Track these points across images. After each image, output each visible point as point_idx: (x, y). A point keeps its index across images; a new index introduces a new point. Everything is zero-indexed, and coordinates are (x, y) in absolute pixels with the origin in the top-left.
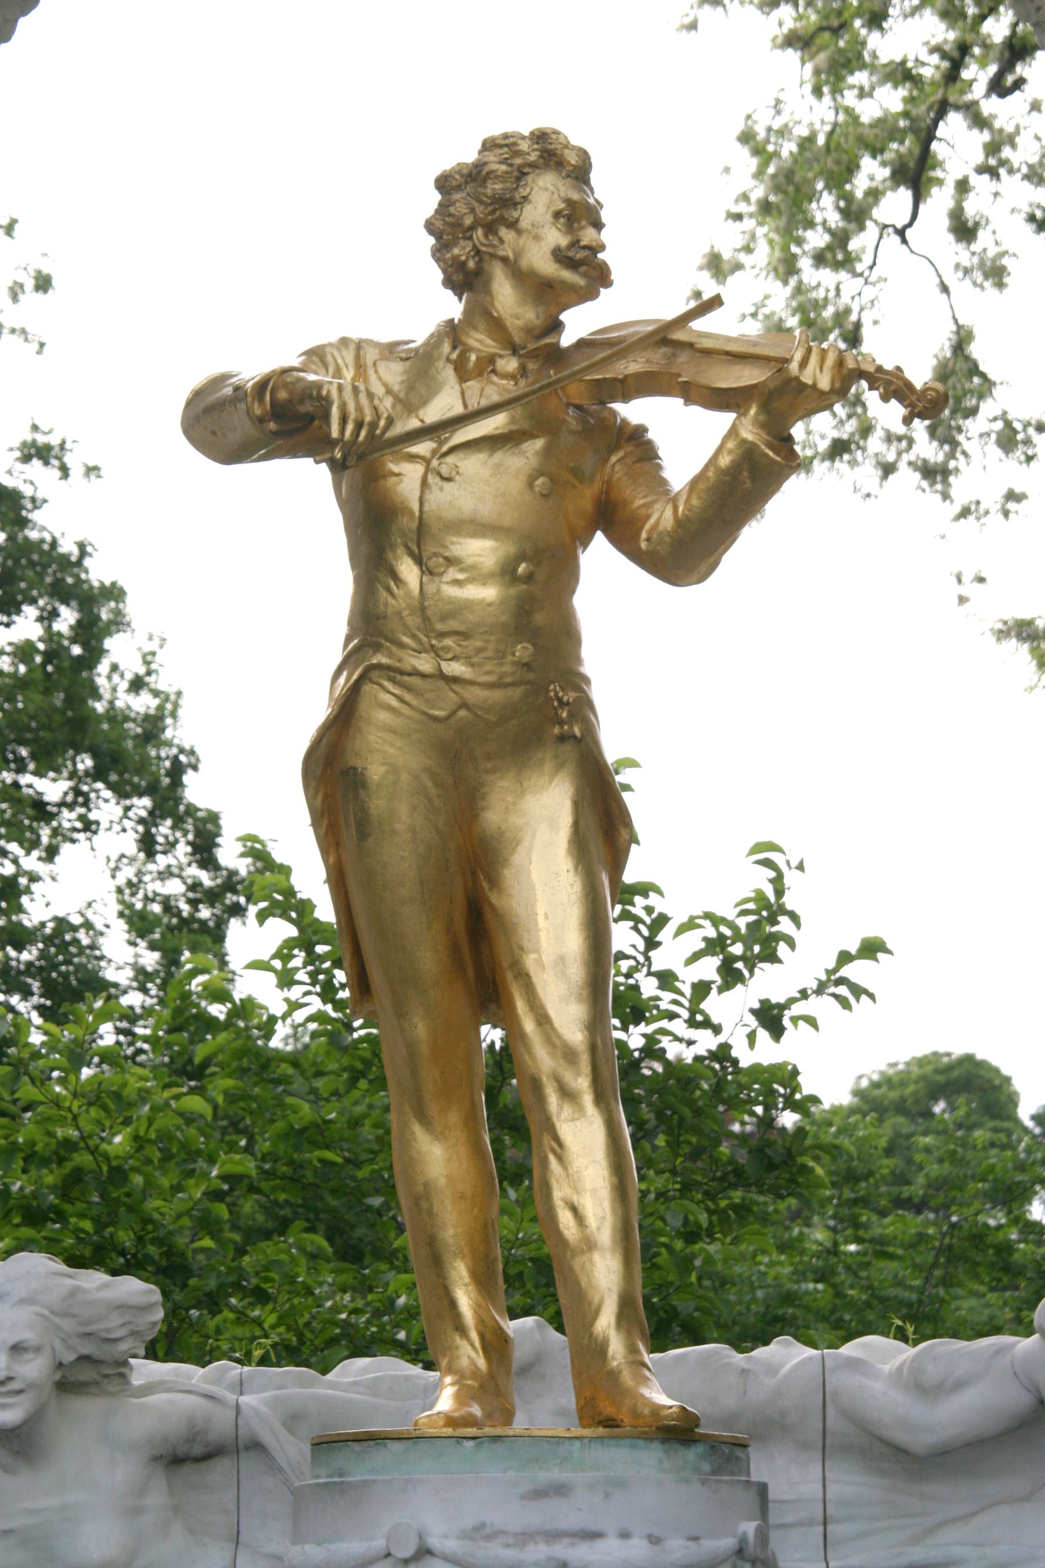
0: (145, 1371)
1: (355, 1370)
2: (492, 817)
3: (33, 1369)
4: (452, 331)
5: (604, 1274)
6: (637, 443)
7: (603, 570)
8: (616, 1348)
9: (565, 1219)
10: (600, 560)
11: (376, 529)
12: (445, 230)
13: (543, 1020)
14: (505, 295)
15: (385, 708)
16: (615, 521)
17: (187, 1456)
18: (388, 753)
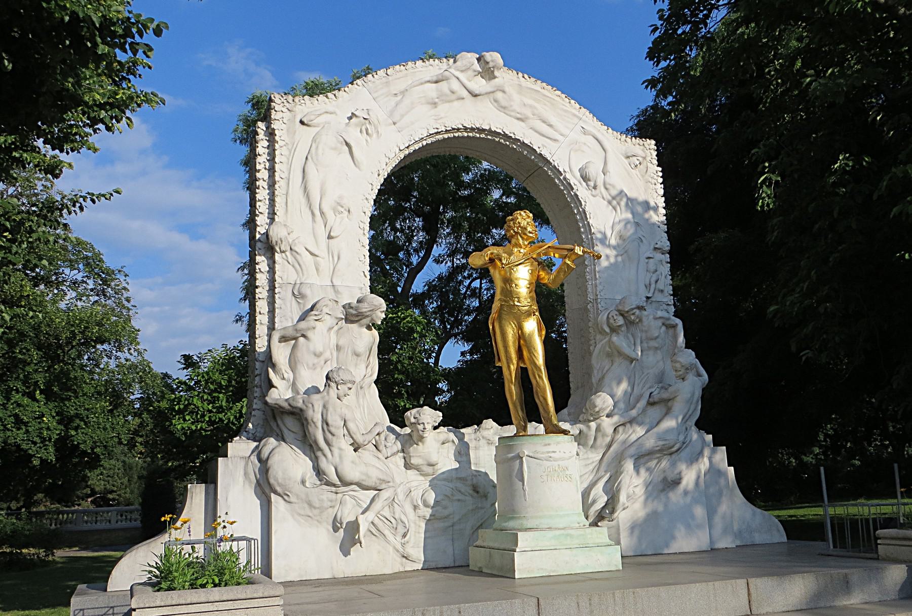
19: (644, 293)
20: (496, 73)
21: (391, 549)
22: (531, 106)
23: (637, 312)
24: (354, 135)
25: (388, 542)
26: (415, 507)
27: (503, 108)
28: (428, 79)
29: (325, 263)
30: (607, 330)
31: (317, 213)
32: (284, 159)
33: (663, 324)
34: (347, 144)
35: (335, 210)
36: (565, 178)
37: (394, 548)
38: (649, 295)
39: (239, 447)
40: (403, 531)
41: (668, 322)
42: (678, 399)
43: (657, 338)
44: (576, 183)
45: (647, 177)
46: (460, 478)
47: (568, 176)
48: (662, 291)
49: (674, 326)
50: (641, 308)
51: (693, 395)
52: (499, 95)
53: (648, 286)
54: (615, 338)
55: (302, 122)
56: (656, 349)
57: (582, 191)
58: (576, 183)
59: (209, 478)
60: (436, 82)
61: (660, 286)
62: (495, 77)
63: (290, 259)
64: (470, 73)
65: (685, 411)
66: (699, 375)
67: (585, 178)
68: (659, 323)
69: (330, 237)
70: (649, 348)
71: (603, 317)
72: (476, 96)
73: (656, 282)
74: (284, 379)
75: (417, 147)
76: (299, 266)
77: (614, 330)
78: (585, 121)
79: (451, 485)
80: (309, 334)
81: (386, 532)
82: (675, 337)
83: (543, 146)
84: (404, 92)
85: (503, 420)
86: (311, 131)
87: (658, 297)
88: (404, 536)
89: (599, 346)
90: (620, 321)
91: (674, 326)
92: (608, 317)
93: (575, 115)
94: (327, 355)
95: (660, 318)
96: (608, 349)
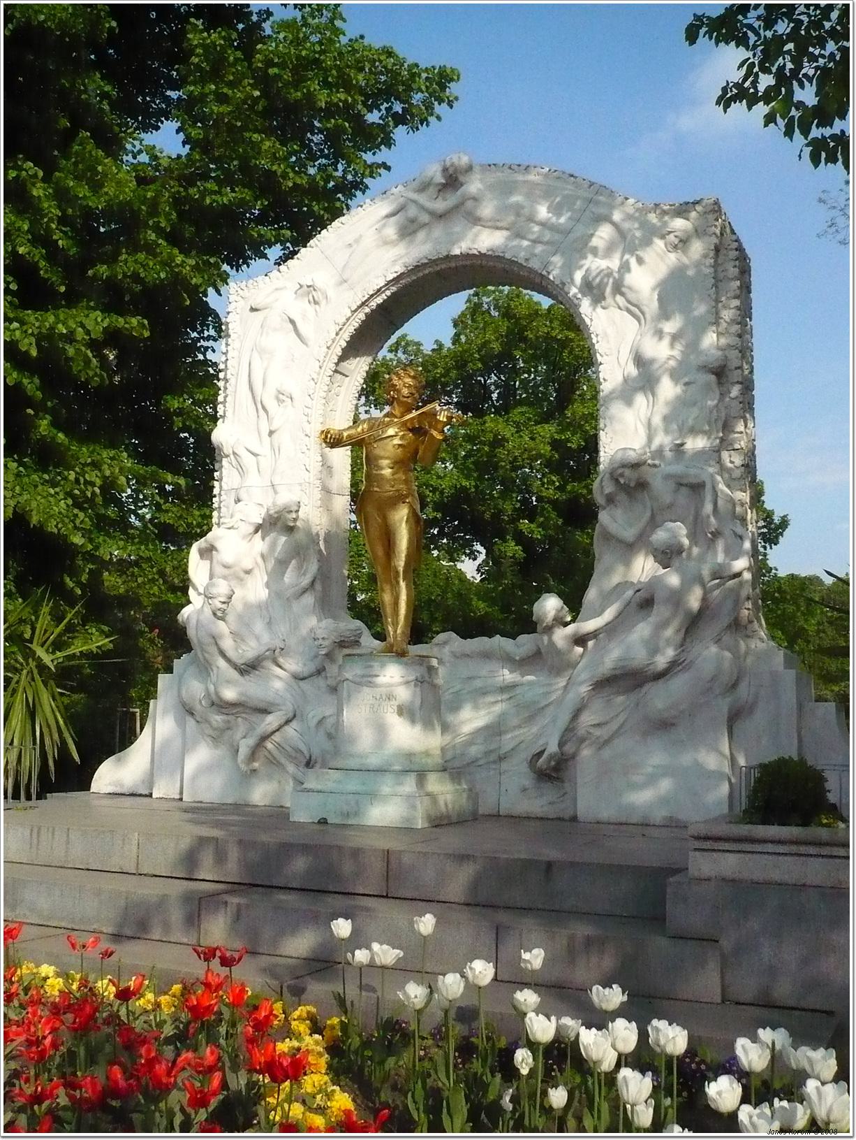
3: (326, 643)
20: (461, 178)
23: (627, 472)
29: (265, 462)
34: (292, 322)
35: (278, 399)
41: (685, 481)
55: (253, 310)
63: (234, 462)
64: (432, 190)
68: (671, 485)
69: (271, 433)
72: (441, 216)
75: (379, 300)
76: (241, 470)
78: (598, 203)
81: (283, 760)
84: (357, 241)
90: (609, 488)
94: (248, 564)
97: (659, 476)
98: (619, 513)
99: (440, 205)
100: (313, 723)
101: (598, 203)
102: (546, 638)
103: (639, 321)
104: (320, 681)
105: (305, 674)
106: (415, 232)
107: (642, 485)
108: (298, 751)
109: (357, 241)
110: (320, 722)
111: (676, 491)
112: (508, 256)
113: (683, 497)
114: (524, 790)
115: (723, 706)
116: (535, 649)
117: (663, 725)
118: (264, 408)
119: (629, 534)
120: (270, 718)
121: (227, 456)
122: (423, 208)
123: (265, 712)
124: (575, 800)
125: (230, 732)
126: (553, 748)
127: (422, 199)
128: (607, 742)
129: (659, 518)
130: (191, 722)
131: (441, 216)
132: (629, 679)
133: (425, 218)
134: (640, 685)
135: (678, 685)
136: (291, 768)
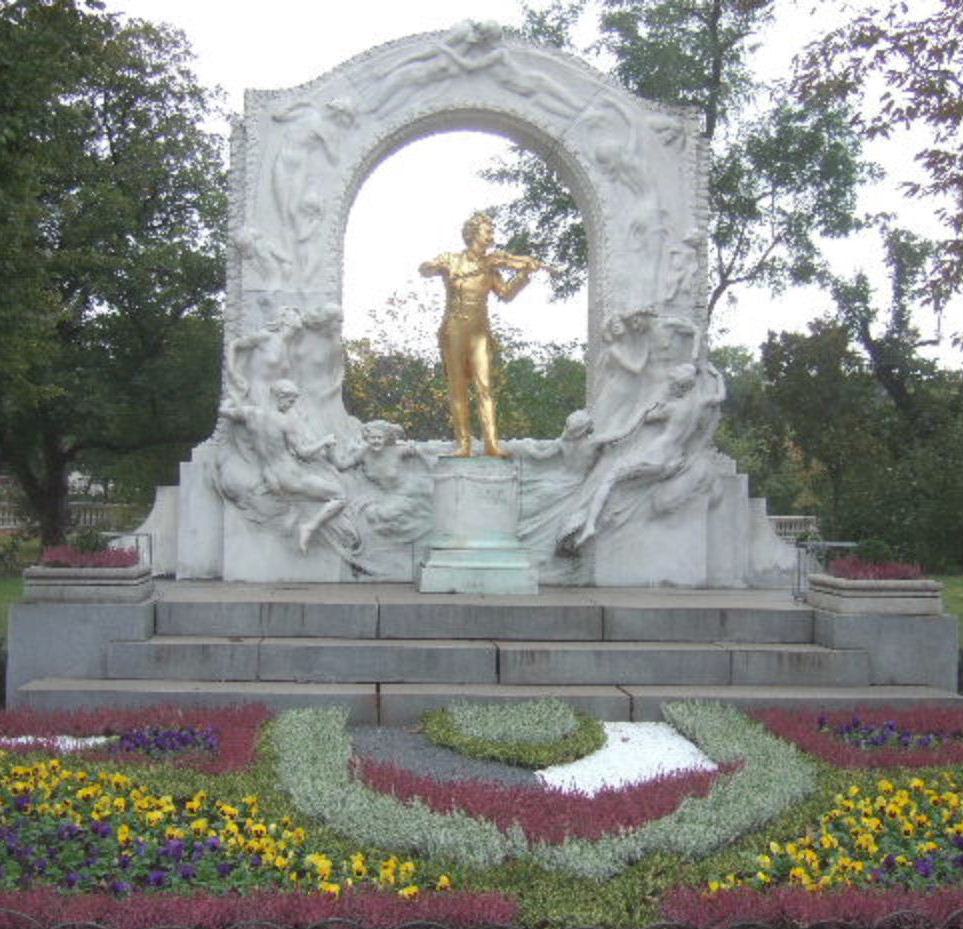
0: (398, 442)
1: (431, 442)
2: (473, 344)
3: (381, 441)
4: (465, 252)
5: (491, 430)
6: (498, 275)
7: (492, 297)
8: (493, 442)
9: (484, 420)
10: (492, 297)
11: (453, 292)
12: (465, 233)
13: (480, 383)
14: (476, 246)
15: (453, 322)
16: (494, 289)
17: (407, 457)
18: (454, 332)
19: (664, 295)
21: (338, 560)
22: (540, 79)
23: (640, 320)
24: (326, 129)
25: (335, 551)
26: (371, 521)
27: (506, 84)
28: (413, 55)
30: (609, 337)
31: (285, 215)
32: (254, 159)
33: (676, 332)
34: (318, 138)
36: (578, 162)
37: (343, 557)
38: (670, 296)
39: (201, 451)
40: (352, 543)
42: (672, 420)
43: (666, 349)
44: (588, 165)
45: (684, 154)
46: (423, 495)
47: (578, 157)
48: (687, 292)
49: (690, 335)
50: (645, 315)
51: (689, 414)
52: (498, 69)
53: (668, 287)
54: (616, 350)
55: (276, 119)
56: (667, 360)
57: (594, 176)
58: (588, 165)
59: (174, 480)
60: (424, 59)
61: (685, 285)
62: (493, 48)
64: (463, 47)
65: (680, 432)
66: (717, 391)
67: (601, 160)
68: (670, 331)
70: (659, 360)
71: (606, 320)
72: (471, 72)
73: (680, 281)
74: (239, 389)
77: (618, 338)
79: (410, 500)
80: (262, 345)
81: (335, 543)
82: (692, 346)
83: (550, 124)
84: (386, 75)
85: (451, 435)
86: (283, 128)
87: (682, 301)
88: (356, 547)
89: (601, 355)
90: (621, 328)
91: (690, 335)
92: (611, 324)
93: (595, 85)
95: (672, 325)
96: (607, 358)
97: (660, 325)
98: (625, 348)
99: (467, 62)
100: (357, 509)
101: (608, 91)
102: (571, 445)
103: (635, 193)
104: (359, 475)
105: (345, 466)
106: (441, 80)
107: (646, 330)
108: (348, 533)
109: (386, 75)
110: (362, 509)
111: (672, 338)
112: (530, 119)
113: (676, 343)
114: (542, 564)
115: (705, 500)
116: (556, 450)
117: (661, 514)
118: (292, 218)
119: (637, 365)
120: (332, 504)
121: (249, 258)
122: (455, 62)
123: (321, 498)
124: (592, 572)
125: (277, 519)
126: (590, 530)
127: (455, 52)
128: (623, 524)
129: (654, 356)
130: (231, 510)
131: (471, 72)
132: (639, 480)
133: (454, 69)
134: (649, 485)
135: (679, 485)
136: (341, 550)
